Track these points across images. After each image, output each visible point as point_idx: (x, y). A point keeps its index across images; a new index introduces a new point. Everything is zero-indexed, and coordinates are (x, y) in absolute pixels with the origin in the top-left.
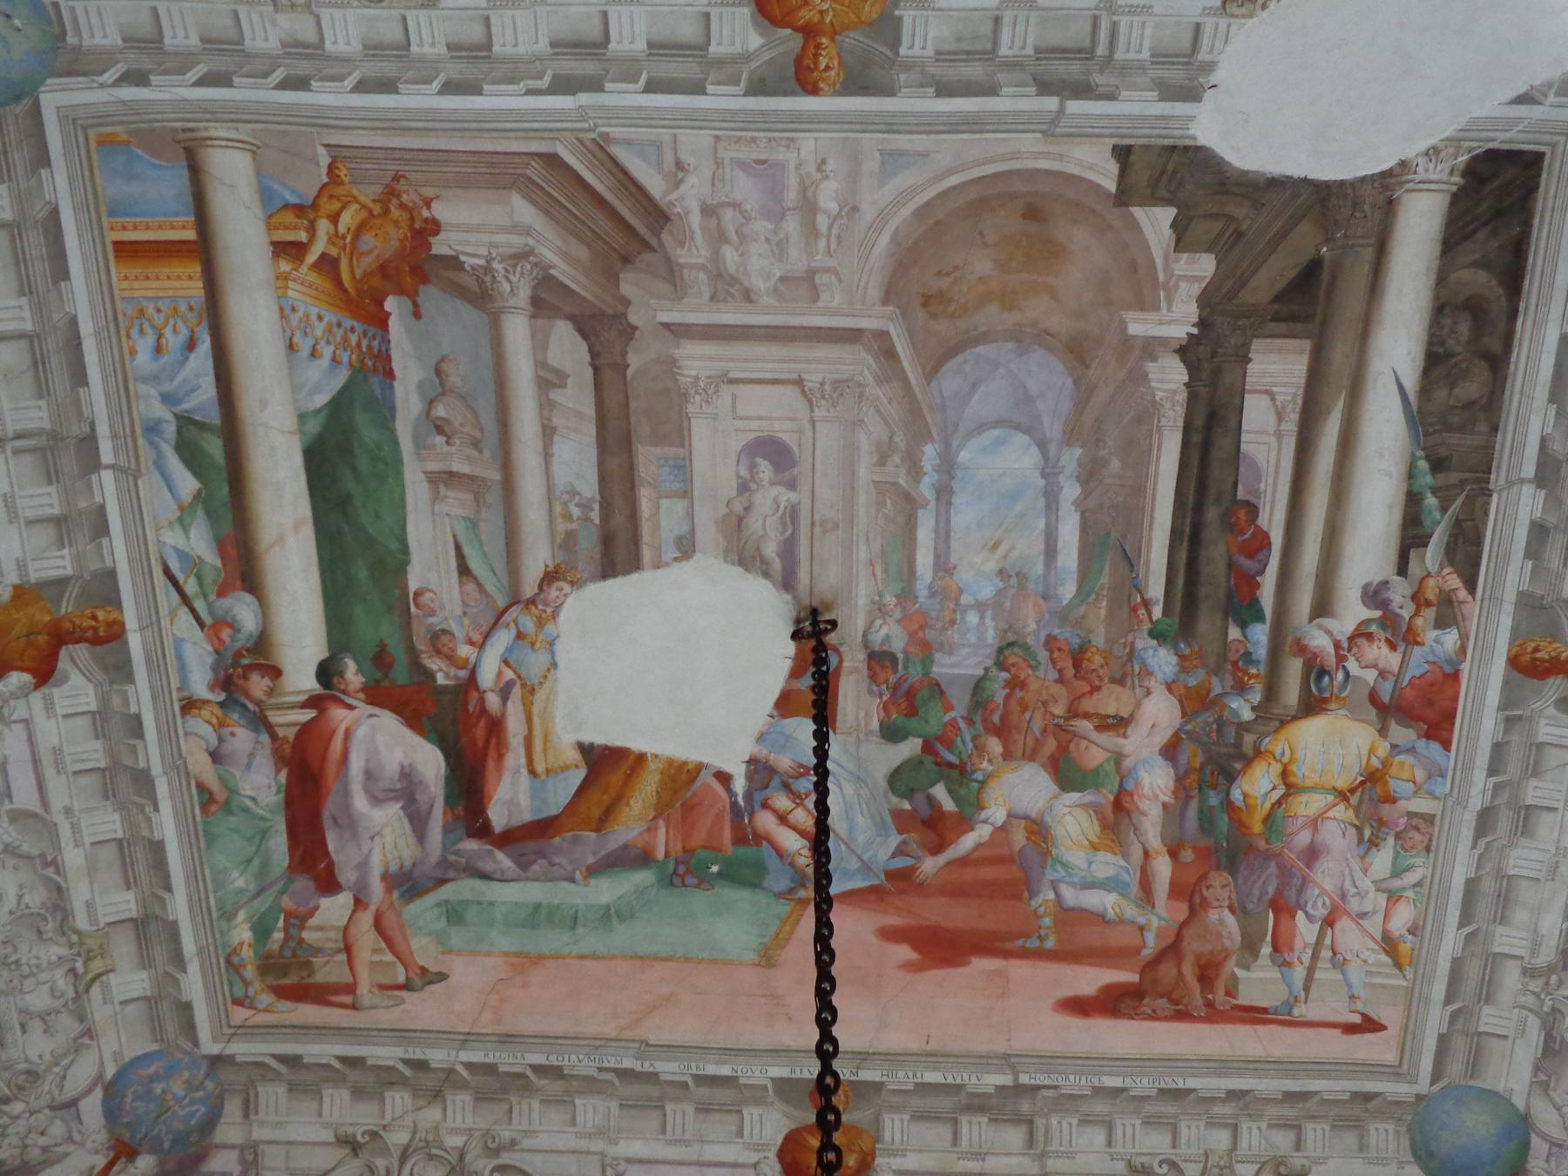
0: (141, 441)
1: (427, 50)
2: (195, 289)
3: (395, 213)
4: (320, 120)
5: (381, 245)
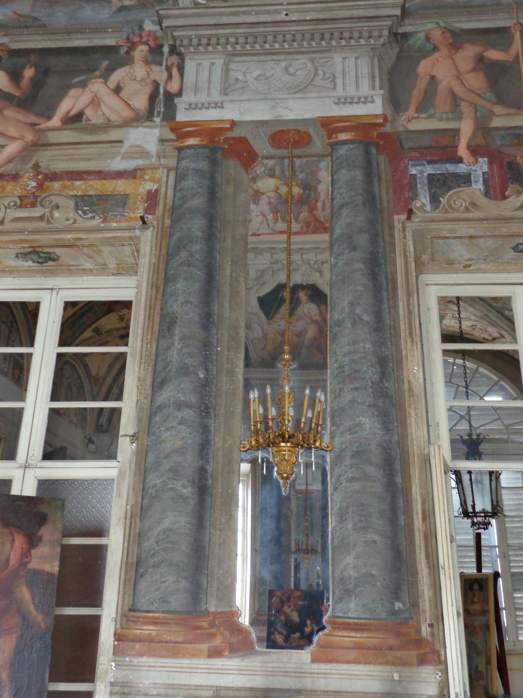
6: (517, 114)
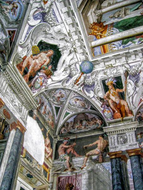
0: (125, 48)
1: (74, 29)
2: (107, 45)
3: (94, 27)
4: (85, 37)
5: (97, 28)
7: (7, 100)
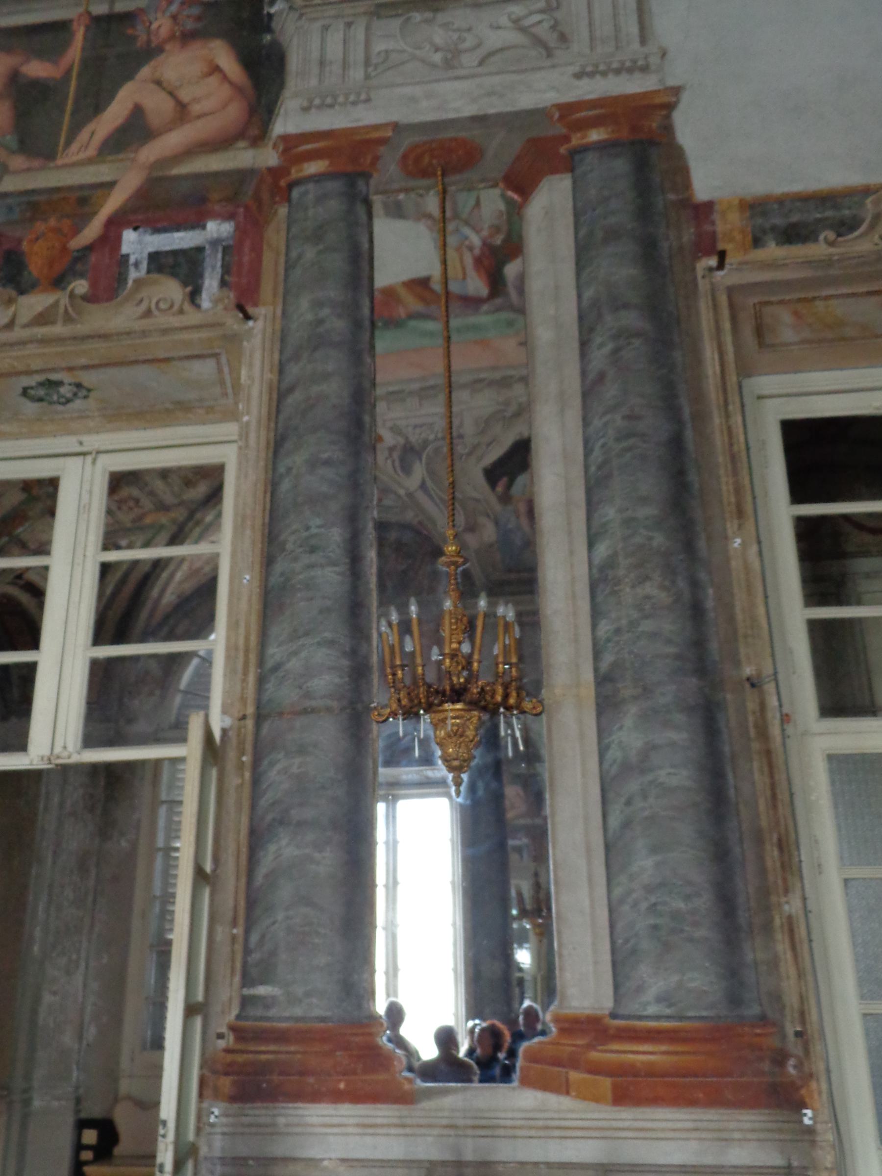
6: (41, 168)
7: (408, 90)
